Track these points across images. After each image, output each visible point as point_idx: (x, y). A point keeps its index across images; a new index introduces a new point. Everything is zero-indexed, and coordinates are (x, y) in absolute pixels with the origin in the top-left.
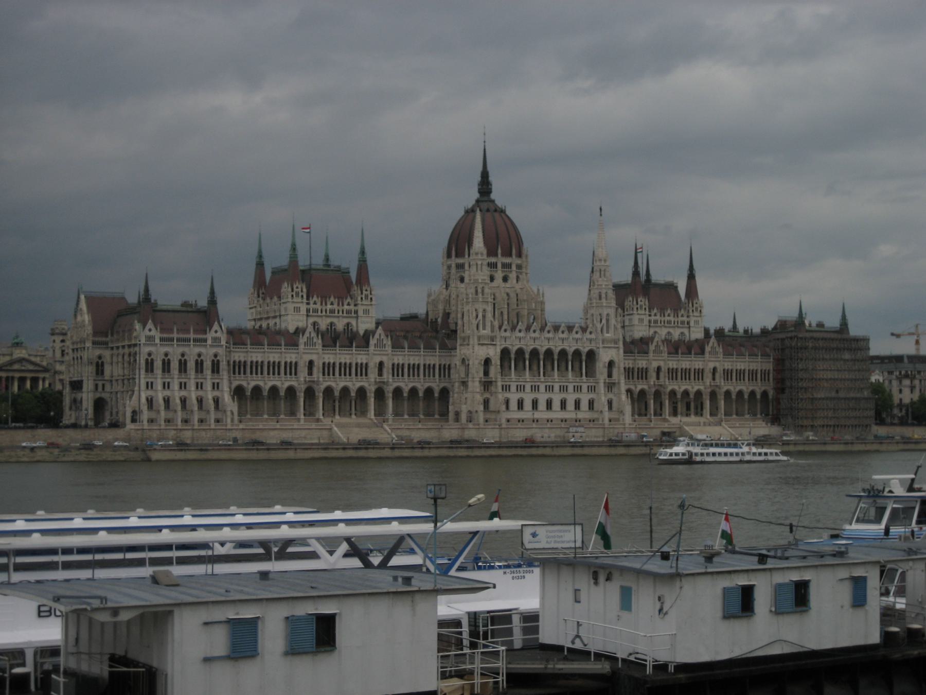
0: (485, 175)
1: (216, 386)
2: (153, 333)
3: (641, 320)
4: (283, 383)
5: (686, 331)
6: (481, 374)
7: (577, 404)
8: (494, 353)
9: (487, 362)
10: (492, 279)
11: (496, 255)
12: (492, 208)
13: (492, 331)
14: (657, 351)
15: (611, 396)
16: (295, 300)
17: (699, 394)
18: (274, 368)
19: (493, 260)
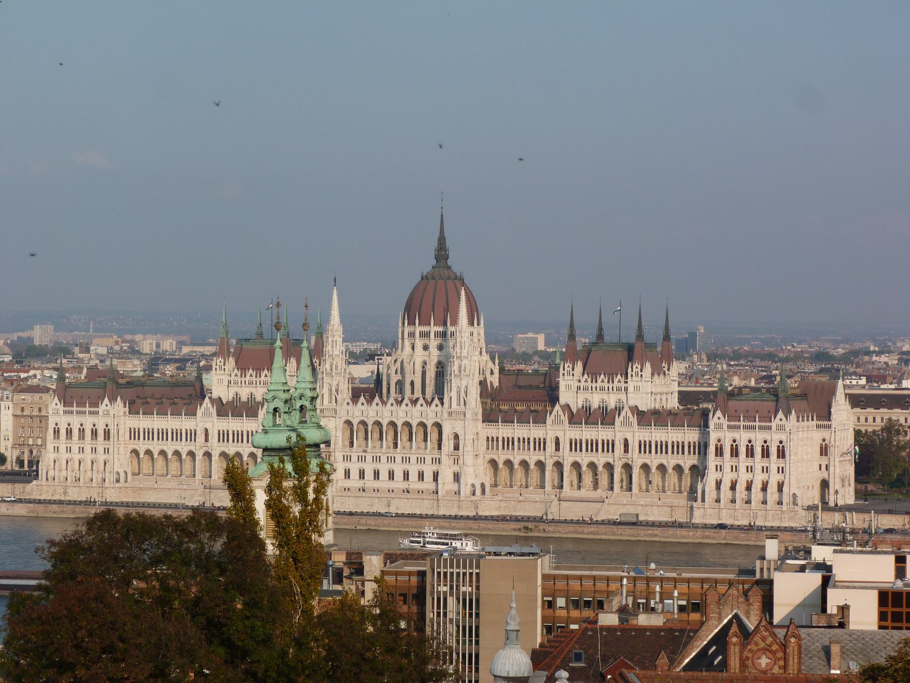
0: (442, 240)
1: (107, 451)
3: (569, 387)
4: (184, 448)
5: (623, 397)
7: (421, 476)
12: (452, 275)
18: (177, 435)
19: (412, 329)
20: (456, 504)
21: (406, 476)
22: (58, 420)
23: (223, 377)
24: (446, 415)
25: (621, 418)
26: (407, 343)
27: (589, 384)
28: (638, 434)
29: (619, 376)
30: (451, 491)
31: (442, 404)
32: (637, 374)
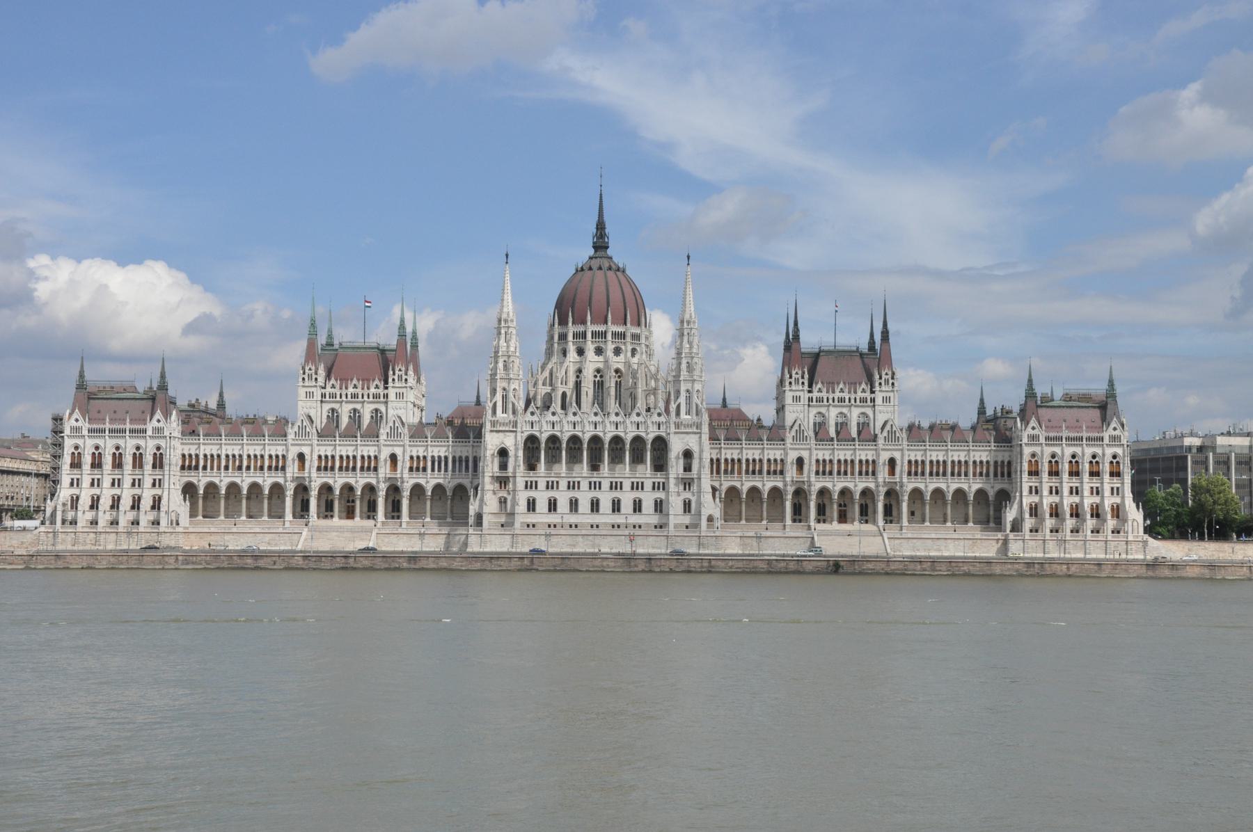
0: (601, 226)
2: (79, 424)
3: (797, 399)
4: (266, 480)
5: (869, 412)
6: (496, 468)
7: (637, 506)
8: (515, 444)
9: (503, 453)
10: (581, 352)
11: (584, 322)
13: (514, 412)
14: (800, 436)
15: (688, 495)
16: (307, 384)
17: (866, 493)
18: (257, 464)
19: (581, 328)
20: (695, 541)
21: (616, 506)
22: (80, 442)
23: (311, 390)
24: (673, 426)
25: (885, 434)
26: (572, 349)
27: (824, 395)
28: (907, 454)
29: (863, 386)
30: (681, 525)
31: (667, 411)
32: (887, 382)
